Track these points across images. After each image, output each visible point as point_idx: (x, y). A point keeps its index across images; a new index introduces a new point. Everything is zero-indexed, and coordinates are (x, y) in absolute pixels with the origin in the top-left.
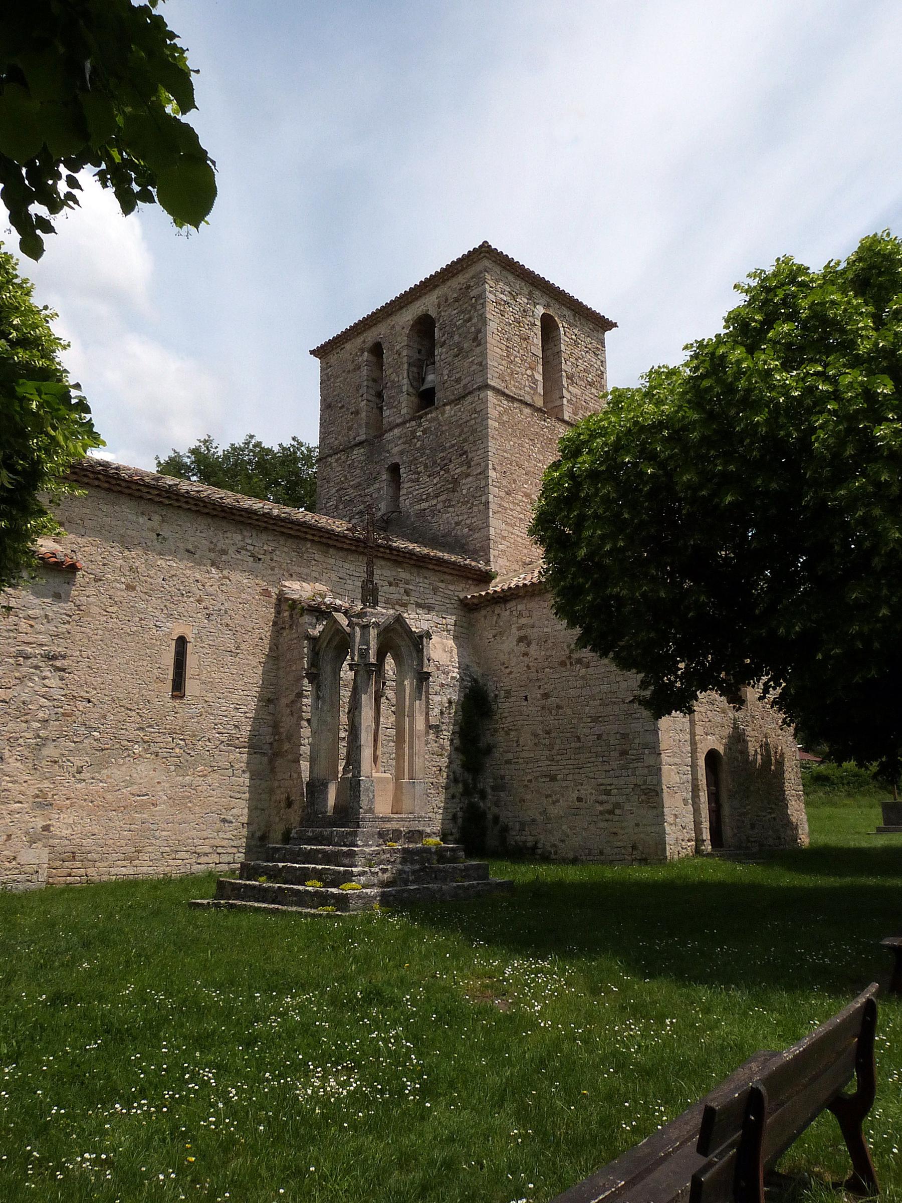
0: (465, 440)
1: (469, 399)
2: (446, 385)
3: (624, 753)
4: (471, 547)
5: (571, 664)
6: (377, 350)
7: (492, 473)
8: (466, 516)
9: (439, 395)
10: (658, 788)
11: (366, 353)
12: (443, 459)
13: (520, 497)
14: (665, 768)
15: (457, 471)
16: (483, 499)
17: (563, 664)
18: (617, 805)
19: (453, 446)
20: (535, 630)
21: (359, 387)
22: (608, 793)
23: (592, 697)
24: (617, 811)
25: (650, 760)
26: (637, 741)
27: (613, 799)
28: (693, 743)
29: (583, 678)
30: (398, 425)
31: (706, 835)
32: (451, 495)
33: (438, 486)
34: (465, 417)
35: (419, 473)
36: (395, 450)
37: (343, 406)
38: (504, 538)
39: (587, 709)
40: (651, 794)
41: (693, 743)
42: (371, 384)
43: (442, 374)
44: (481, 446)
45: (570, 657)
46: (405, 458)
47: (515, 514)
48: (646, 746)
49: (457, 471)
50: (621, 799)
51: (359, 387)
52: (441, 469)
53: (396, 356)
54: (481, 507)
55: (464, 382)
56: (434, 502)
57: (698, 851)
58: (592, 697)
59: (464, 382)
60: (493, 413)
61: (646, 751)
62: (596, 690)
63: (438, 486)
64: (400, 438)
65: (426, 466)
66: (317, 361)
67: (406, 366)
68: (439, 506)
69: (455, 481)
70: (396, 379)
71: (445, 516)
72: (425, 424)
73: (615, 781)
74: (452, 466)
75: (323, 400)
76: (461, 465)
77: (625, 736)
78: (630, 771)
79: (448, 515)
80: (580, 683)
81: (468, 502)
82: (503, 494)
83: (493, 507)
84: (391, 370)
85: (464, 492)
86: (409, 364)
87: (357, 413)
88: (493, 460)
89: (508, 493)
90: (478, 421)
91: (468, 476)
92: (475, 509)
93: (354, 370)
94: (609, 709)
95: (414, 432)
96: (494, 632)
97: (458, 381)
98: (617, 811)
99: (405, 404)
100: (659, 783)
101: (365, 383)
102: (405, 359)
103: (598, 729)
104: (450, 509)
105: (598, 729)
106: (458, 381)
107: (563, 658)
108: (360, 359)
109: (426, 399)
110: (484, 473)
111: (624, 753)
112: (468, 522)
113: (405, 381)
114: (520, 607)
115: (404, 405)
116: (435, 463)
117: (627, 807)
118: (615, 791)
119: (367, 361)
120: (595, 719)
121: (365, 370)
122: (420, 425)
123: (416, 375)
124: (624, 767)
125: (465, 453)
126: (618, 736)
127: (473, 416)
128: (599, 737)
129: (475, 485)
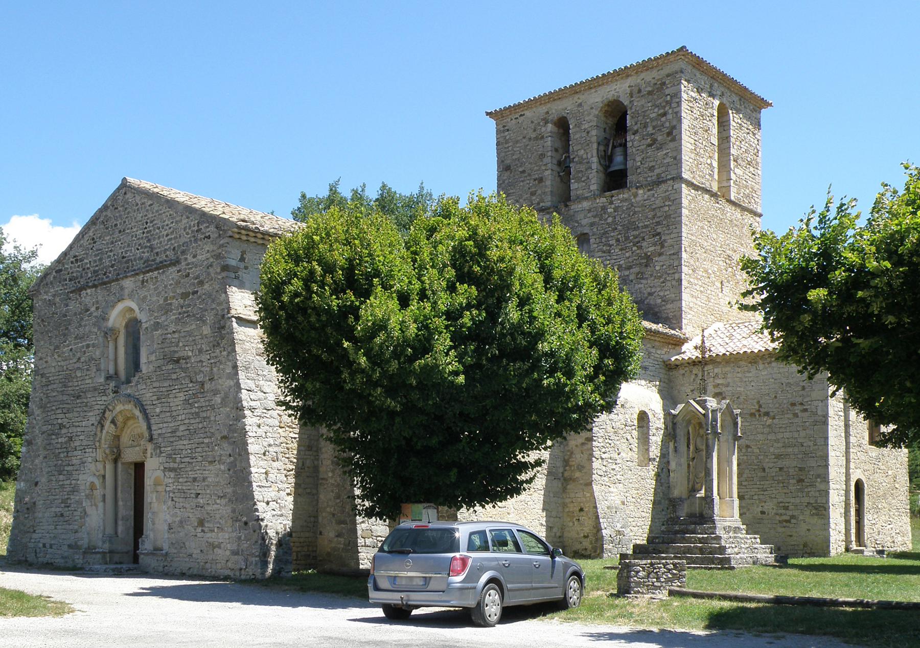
0: (658, 223)
1: (663, 187)
2: (639, 171)
3: (800, 481)
4: (664, 316)
5: (760, 415)
6: (563, 125)
7: (684, 255)
8: (659, 289)
9: (630, 178)
10: (826, 506)
11: (550, 125)
12: (636, 237)
13: (701, 273)
14: (831, 492)
15: (652, 249)
16: (677, 276)
17: (753, 415)
18: (793, 517)
19: (646, 226)
20: (729, 388)
21: (542, 156)
22: (787, 508)
23: (777, 441)
24: (793, 521)
25: (822, 487)
26: (811, 473)
27: (790, 513)
28: (848, 475)
29: (769, 426)
30: (586, 198)
31: (853, 538)
32: (644, 269)
33: (630, 260)
34: (659, 203)
35: (610, 246)
36: (584, 222)
37: (524, 172)
38: (691, 308)
39: (772, 450)
40: (822, 510)
41: (848, 475)
42: (554, 154)
43: (634, 160)
44: (675, 231)
45: (759, 411)
46: (595, 230)
47: (698, 287)
48: (819, 476)
49: (652, 249)
50: (795, 514)
51: (542, 156)
52: (634, 245)
53: (584, 134)
54: (674, 283)
55: (657, 171)
56: (627, 273)
57: (847, 550)
58: (777, 441)
59: (657, 171)
60: (685, 202)
61: (819, 480)
62: (780, 436)
63: (630, 260)
64: (589, 211)
65: (618, 240)
66: (492, 123)
67: (595, 146)
68: (631, 277)
69: (648, 258)
70: (585, 156)
71: (637, 286)
72: (617, 203)
73: (792, 500)
74: (644, 244)
75: (501, 162)
76: (655, 244)
77: (801, 469)
78: (804, 494)
79: (640, 286)
80: (766, 430)
81: (660, 277)
82: (690, 272)
83: (684, 283)
84: (579, 147)
85: (658, 268)
86: (599, 144)
87: (541, 180)
88: (685, 243)
89: (694, 271)
90: (672, 208)
91: (660, 254)
92: (669, 284)
93: (536, 139)
94: (790, 450)
95: (604, 208)
96: (692, 388)
97: (652, 169)
98: (793, 521)
99: (595, 180)
100: (827, 501)
101: (549, 154)
102: (594, 139)
103: (780, 463)
104: (644, 281)
105: (780, 463)
106: (652, 169)
107: (753, 411)
108: (543, 129)
109: (615, 180)
110: (678, 254)
111: (800, 481)
112: (662, 294)
113: (595, 159)
114: (716, 370)
115: (593, 181)
116: (627, 238)
117: (801, 518)
118: (791, 507)
119: (551, 132)
120: (778, 457)
121: (549, 142)
122: (611, 203)
123: (603, 153)
124: (801, 490)
125: (659, 234)
126: (797, 469)
127: (667, 203)
128: (781, 469)
129: (667, 263)
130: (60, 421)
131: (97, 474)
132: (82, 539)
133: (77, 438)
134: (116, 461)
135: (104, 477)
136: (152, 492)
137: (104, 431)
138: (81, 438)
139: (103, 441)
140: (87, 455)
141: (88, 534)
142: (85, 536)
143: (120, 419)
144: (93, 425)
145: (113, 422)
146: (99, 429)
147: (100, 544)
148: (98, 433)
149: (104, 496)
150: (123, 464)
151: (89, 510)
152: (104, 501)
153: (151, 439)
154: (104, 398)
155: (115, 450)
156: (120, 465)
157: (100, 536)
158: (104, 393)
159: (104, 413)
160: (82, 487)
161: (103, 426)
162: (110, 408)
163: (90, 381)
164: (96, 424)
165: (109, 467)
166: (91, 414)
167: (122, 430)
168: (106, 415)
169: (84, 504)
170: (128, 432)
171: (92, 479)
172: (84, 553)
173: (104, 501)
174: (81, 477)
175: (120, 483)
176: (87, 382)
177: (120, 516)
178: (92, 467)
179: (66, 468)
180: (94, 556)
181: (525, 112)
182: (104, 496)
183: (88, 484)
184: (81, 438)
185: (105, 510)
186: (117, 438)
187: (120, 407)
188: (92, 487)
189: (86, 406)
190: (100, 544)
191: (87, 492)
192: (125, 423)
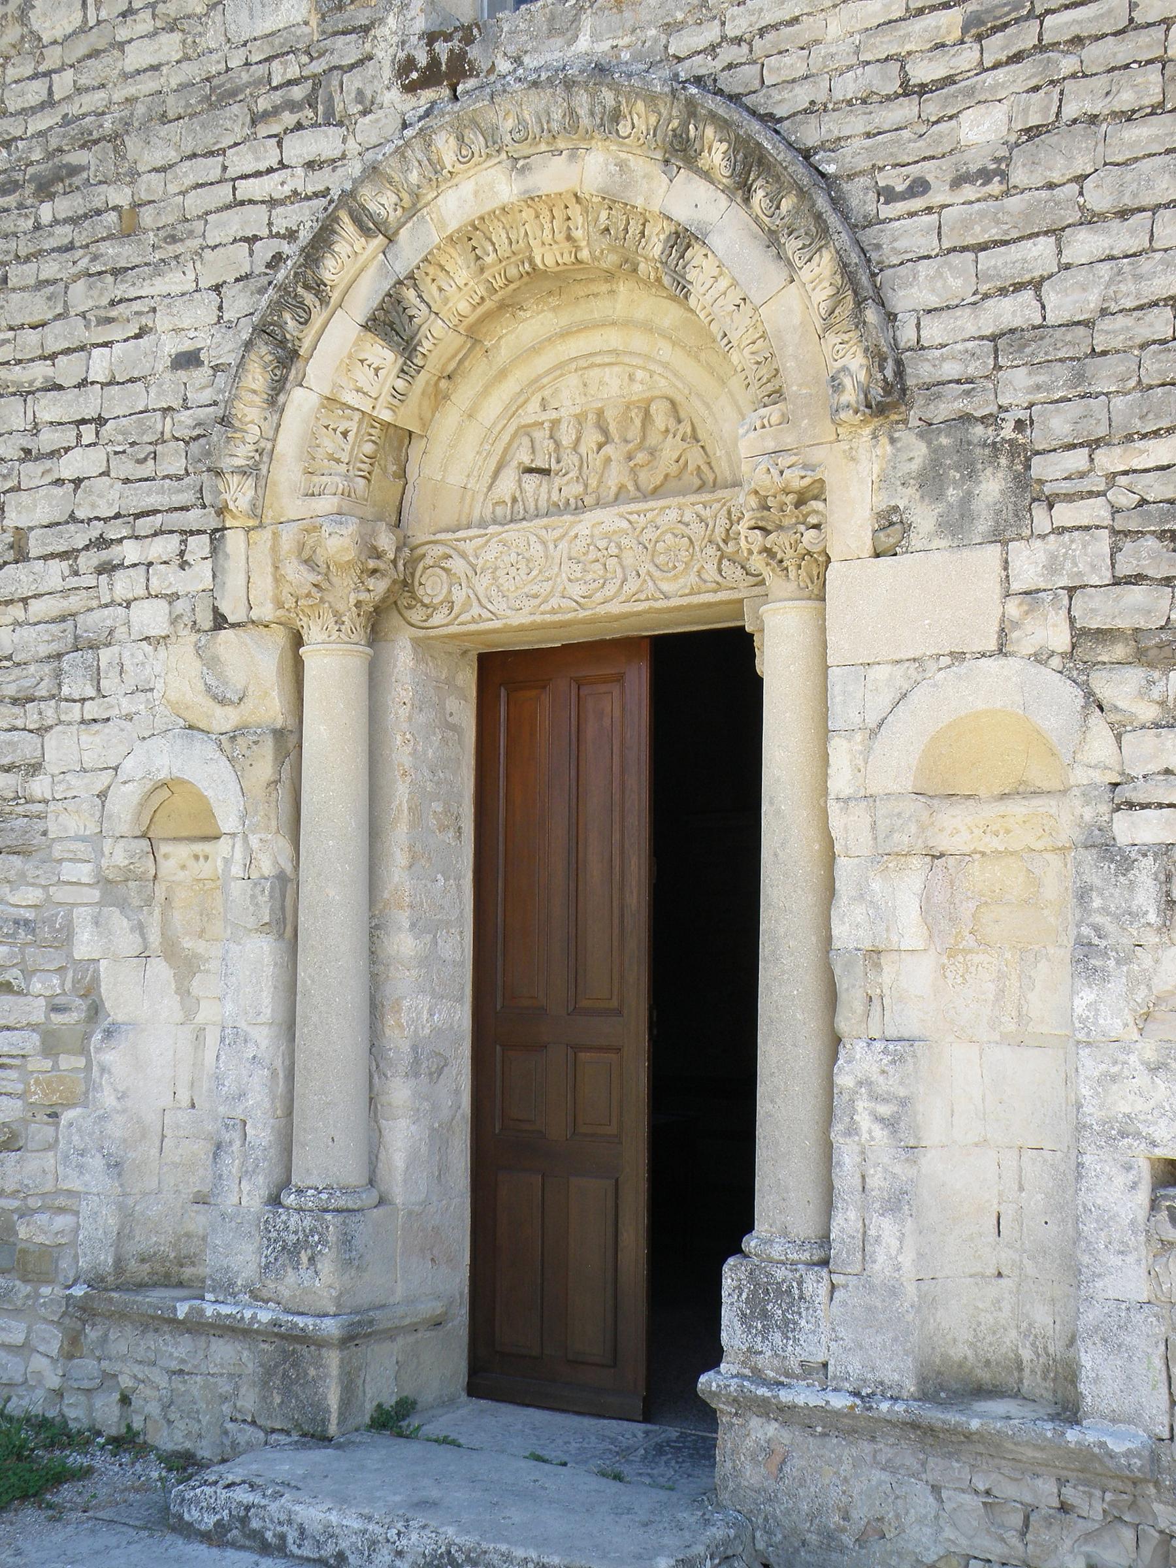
131: (224, 719)
132: (61, 1202)
133: (32, 472)
134: (376, 624)
135: (288, 742)
136: (886, 857)
137: (301, 402)
138: (69, 467)
139: (287, 471)
140: (124, 585)
141: (115, 1166)
142: (92, 1178)
143: (456, 292)
144: (188, 360)
145: (391, 322)
146: (257, 378)
147: (244, 1258)
148: (250, 411)
149: (286, 886)
150: (422, 647)
151: (137, 994)
152: (286, 926)
153: (890, 398)
154: (323, 143)
155: (386, 542)
156: (402, 656)
157: (249, 1195)
158: (318, 103)
159: (323, 239)
160: (69, 823)
161: (288, 357)
162: (381, 202)
163: (170, 46)
164: (224, 349)
165: (331, 663)
166: (175, 281)
167: (439, 398)
168: (331, 270)
169: (85, 945)
170: (493, 408)
171: (165, 758)
172: (83, 1312)
173: (286, 926)
174: (59, 749)
175: (401, 793)
176: (135, 58)
177: (398, 1038)
178: (178, 674)
180: (179, 1349)
182: (286, 886)
183: (125, 801)
184: (69, 467)
185: (290, 988)
186: (397, 442)
187: (473, 190)
188: (173, 816)
189: (129, 230)
190: (244, 1258)
191: (118, 856)
192: (474, 335)
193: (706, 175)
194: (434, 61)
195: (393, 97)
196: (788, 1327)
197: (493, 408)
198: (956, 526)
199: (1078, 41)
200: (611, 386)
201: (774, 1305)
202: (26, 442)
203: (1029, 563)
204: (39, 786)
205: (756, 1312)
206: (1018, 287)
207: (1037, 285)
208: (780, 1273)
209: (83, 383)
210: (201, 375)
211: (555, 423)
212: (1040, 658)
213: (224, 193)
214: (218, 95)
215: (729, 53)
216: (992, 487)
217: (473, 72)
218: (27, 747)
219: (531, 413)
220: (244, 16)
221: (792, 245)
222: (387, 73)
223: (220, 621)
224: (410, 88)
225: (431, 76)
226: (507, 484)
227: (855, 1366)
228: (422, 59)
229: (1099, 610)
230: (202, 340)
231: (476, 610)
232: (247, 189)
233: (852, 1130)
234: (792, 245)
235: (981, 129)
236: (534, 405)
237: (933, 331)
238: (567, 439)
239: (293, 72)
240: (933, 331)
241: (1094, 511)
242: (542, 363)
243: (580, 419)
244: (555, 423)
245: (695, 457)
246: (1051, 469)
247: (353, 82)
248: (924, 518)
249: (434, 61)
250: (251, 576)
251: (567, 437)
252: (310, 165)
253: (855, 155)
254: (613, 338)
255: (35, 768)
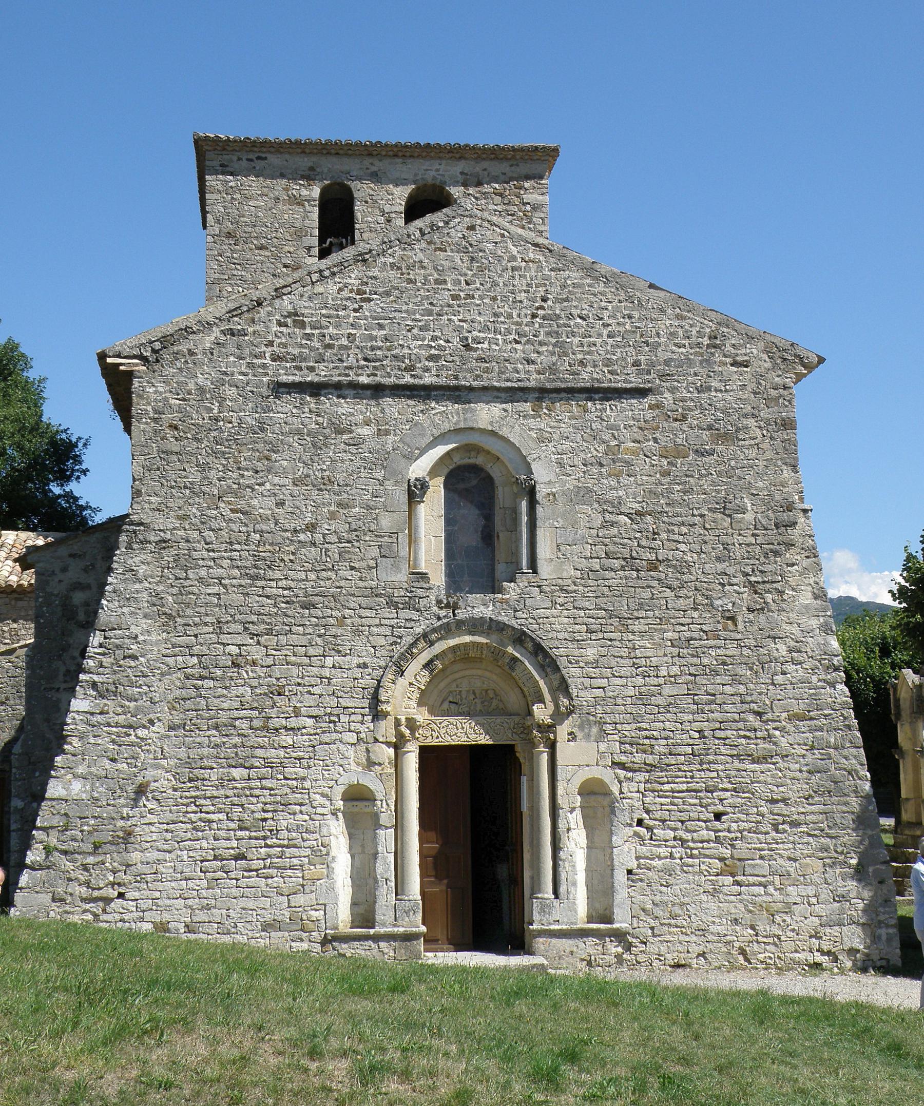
130: (234, 650)
154: (415, 615)
179: (259, 752)
181: (268, 156)
193: (525, 648)
194: (448, 603)
195: (435, 609)
196: (549, 914)
197: (442, 685)
198: (588, 737)
199: (611, 640)
200: (478, 684)
201: (546, 908)
202: (299, 680)
203: (603, 747)
204: (307, 784)
205: (542, 911)
206: (599, 688)
207: (603, 688)
208: (548, 901)
209: (323, 667)
210: (369, 670)
211: (460, 691)
212: (605, 766)
213: (377, 621)
214: (374, 593)
215: (531, 621)
216: (595, 730)
217: (460, 608)
218: (302, 772)
219: (453, 687)
220: (384, 575)
221: (548, 670)
222: (434, 602)
223: (376, 740)
224: (441, 608)
225: (448, 606)
226: (446, 705)
227: (566, 920)
228: (445, 602)
229: (617, 760)
230: (367, 660)
231: (440, 739)
232: (383, 622)
233: (565, 868)
234: (548, 670)
235: (591, 653)
236: (454, 685)
237: (581, 694)
238: (464, 696)
239: (402, 593)
240: (581, 694)
241: (616, 737)
242: (457, 675)
243: (468, 691)
244: (460, 691)
245: (501, 706)
246: (609, 728)
247: (423, 602)
248: (579, 735)
249: (448, 603)
250: (386, 729)
251: (464, 695)
252: (406, 620)
253: (562, 651)
254: (479, 672)
255: (304, 779)
